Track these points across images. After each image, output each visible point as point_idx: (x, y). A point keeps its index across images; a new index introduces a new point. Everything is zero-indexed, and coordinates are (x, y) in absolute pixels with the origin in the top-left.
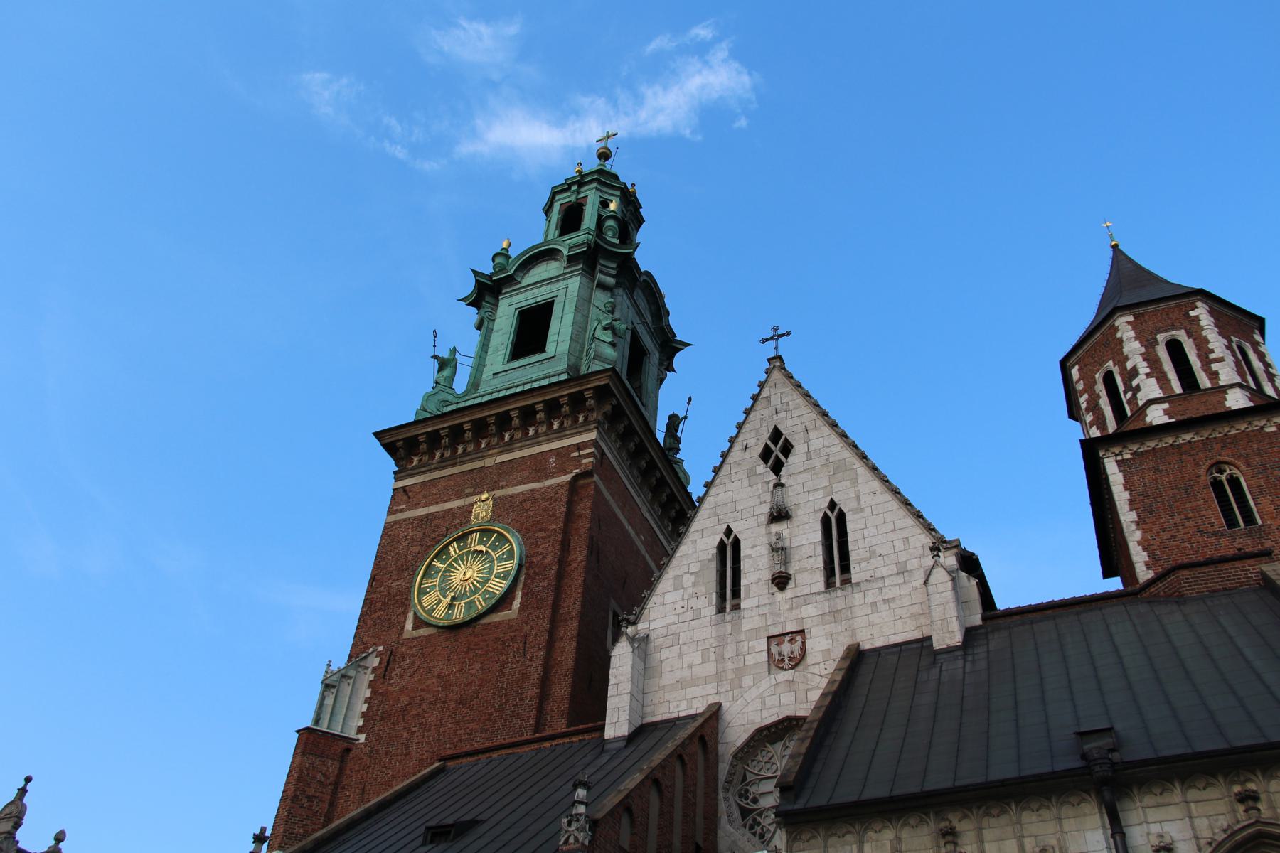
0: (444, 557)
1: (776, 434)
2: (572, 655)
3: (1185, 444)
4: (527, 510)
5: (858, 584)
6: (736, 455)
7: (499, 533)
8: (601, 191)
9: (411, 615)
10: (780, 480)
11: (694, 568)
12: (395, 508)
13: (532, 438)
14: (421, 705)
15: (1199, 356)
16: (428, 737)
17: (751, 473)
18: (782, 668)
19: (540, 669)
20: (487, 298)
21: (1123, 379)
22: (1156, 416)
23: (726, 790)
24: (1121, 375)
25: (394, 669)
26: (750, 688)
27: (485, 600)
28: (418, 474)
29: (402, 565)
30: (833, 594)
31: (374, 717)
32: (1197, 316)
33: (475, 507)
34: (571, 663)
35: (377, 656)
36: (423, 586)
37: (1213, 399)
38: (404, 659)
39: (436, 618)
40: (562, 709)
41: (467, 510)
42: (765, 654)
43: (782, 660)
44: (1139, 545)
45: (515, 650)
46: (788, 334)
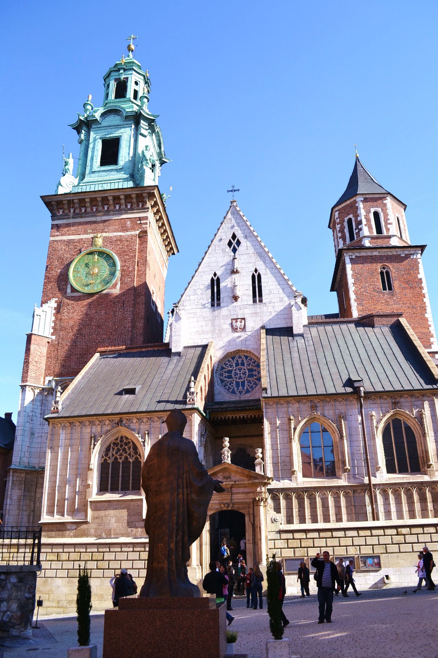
1: (234, 236)
2: (143, 310)
4: (119, 245)
5: (265, 304)
8: (135, 75)
9: (69, 286)
10: (235, 256)
11: (202, 287)
12: (54, 234)
17: (224, 251)
18: (237, 332)
20: (84, 128)
21: (356, 224)
22: (367, 243)
23: (216, 373)
25: (64, 309)
26: (225, 337)
28: (63, 219)
29: (61, 262)
30: (256, 306)
34: (143, 314)
38: (69, 306)
43: (237, 329)
46: (238, 190)
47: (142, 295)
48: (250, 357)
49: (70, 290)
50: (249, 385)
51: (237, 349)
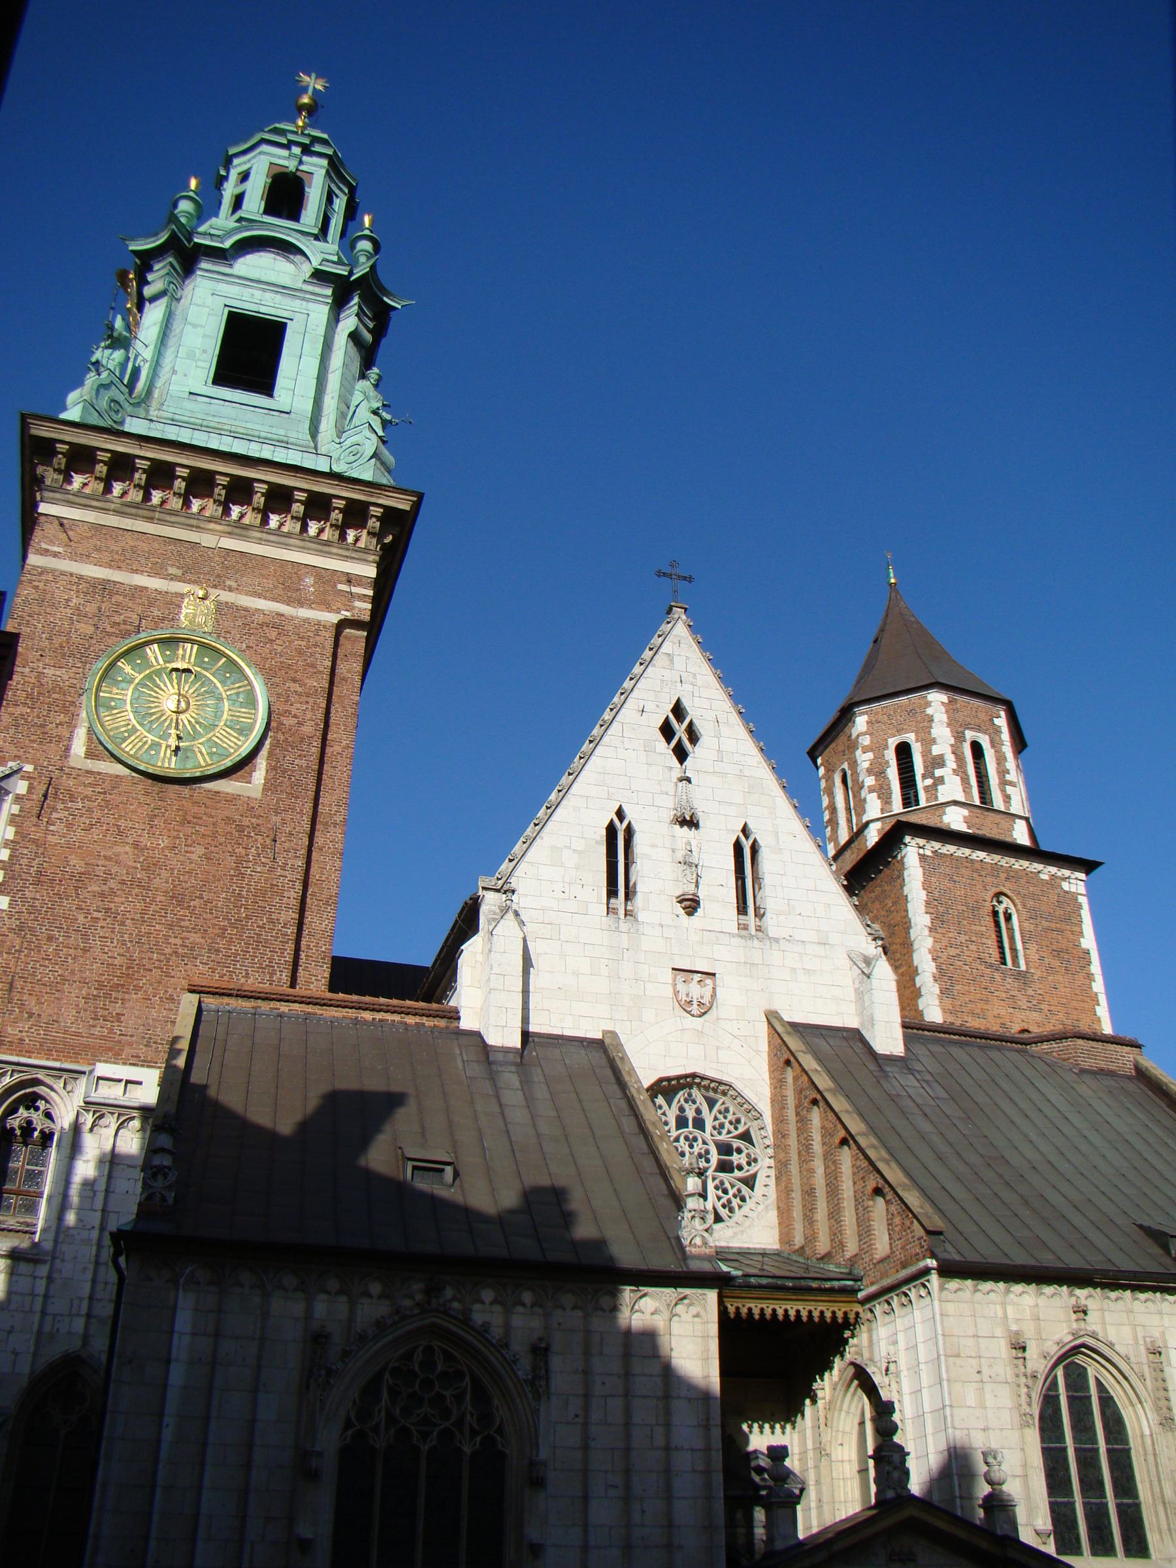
0: (139, 661)
1: (678, 710)
3: (977, 861)
4: (272, 641)
5: (777, 940)
6: (628, 713)
7: (231, 661)
12: (44, 546)
13: (271, 532)
14: (105, 881)
15: (998, 772)
16: (122, 934)
17: (649, 749)
18: (689, 1012)
19: (299, 886)
21: (924, 762)
24: (923, 756)
25: (54, 809)
27: (211, 754)
28: (86, 506)
30: (749, 942)
31: (24, 876)
32: (1000, 727)
33: (186, 600)
35: (23, 778)
36: (101, 694)
37: (1004, 822)
38: (73, 798)
39: (127, 752)
40: (323, 949)
41: (174, 602)
42: (669, 991)
43: (690, 1003)
44: (930, 953)
45: (259, 845)
46: (689, 579)
47: (335, 825)
48: (723, 1103)
49: (84, 749)
50: (719, 1198)
51: (689, 1071)
